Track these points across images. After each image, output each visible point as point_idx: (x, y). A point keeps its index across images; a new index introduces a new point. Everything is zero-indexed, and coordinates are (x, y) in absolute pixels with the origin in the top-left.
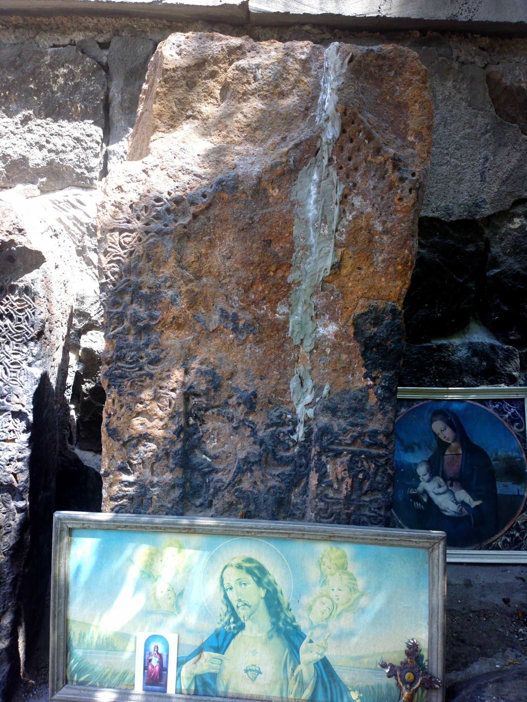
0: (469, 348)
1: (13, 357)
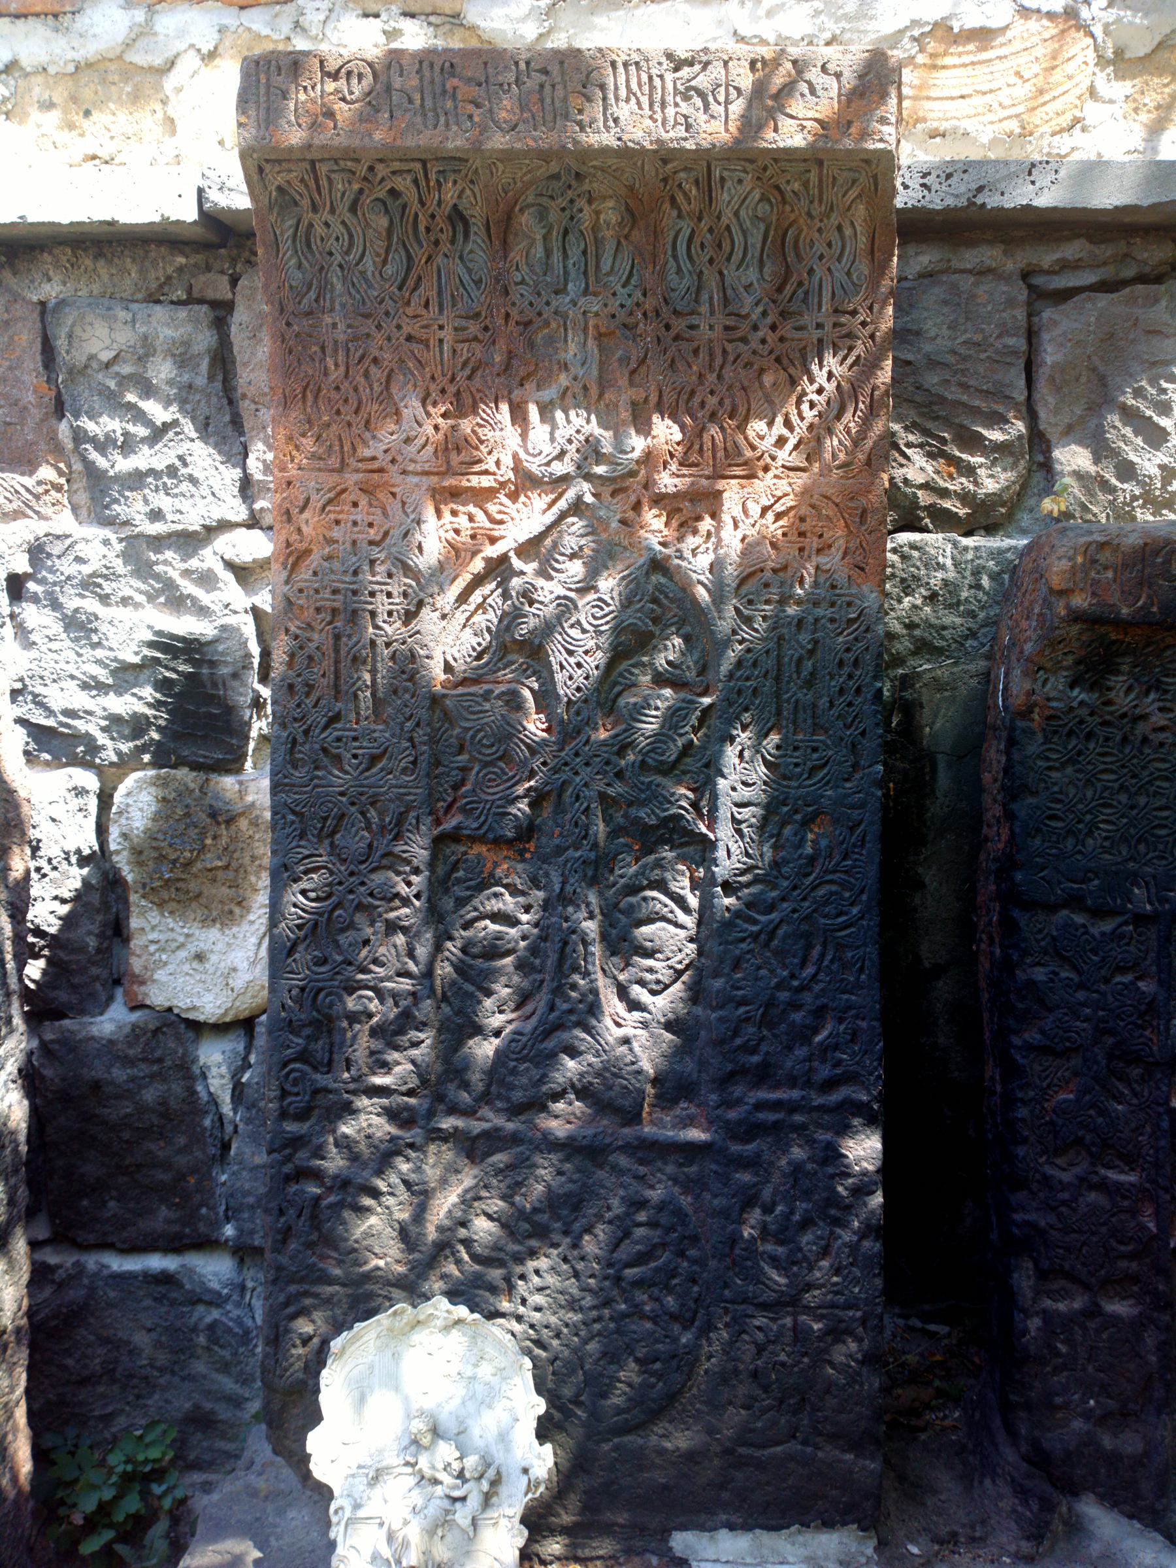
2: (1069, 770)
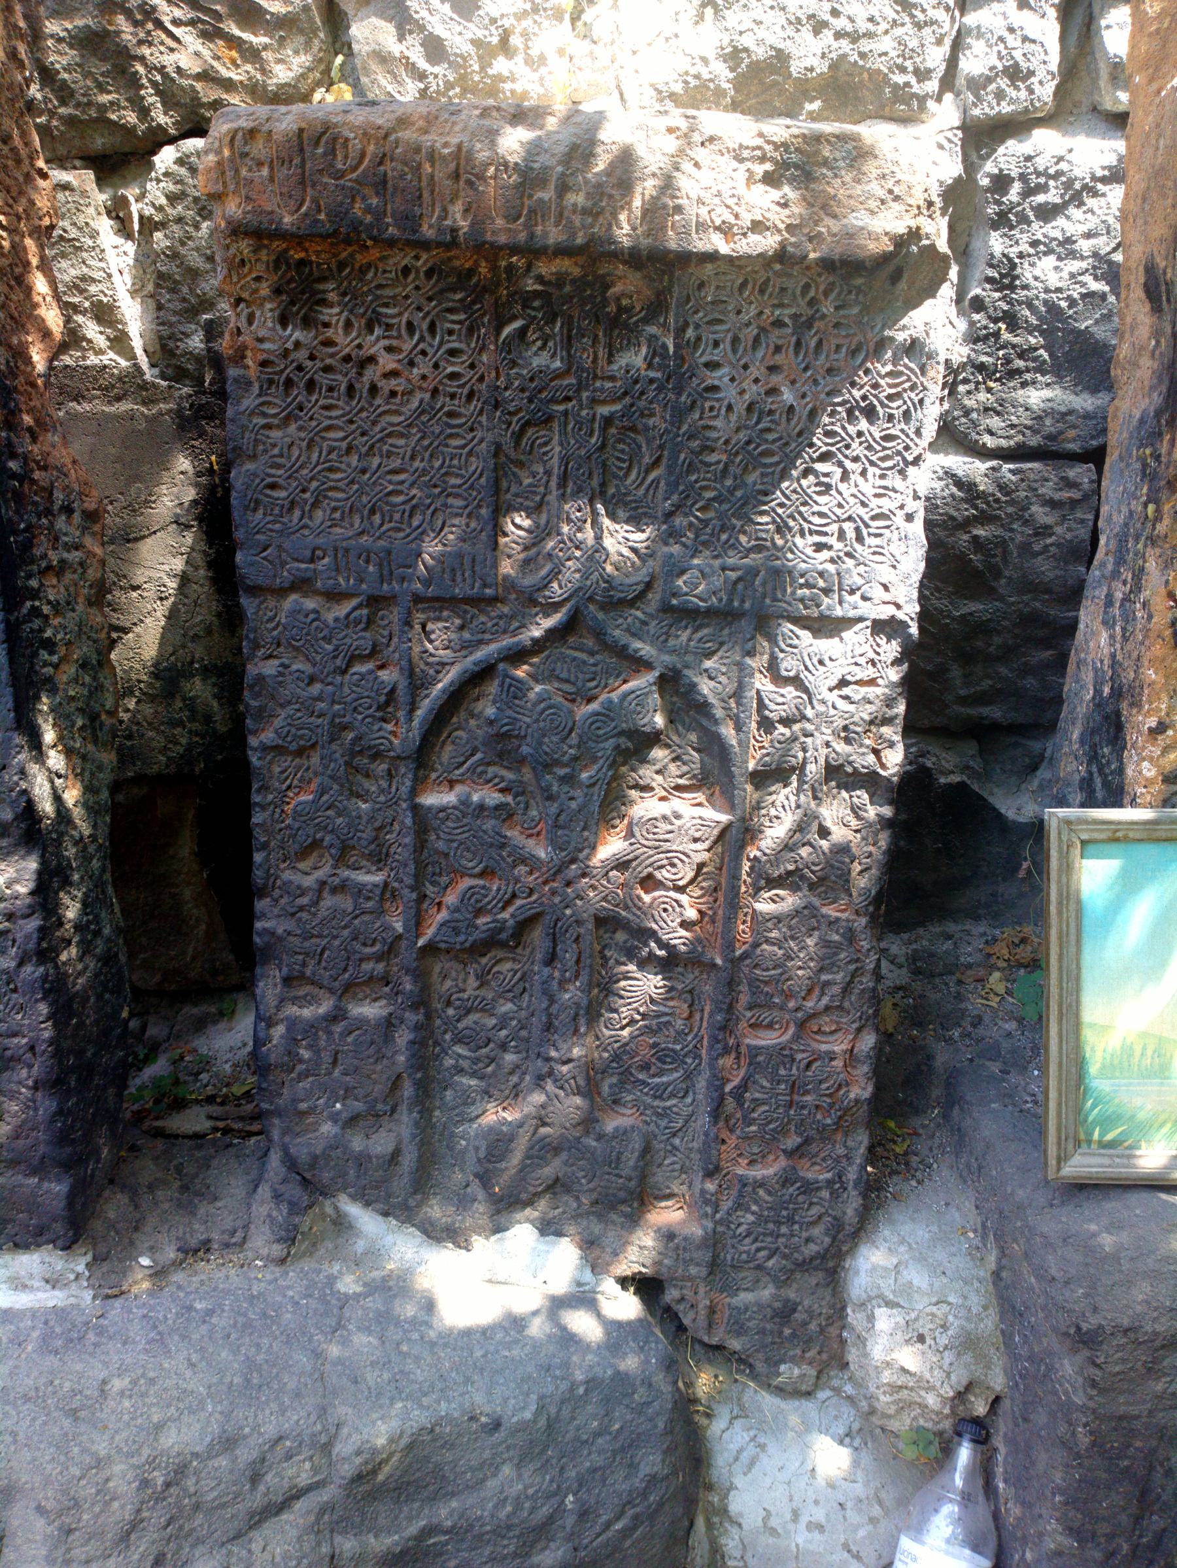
1: (874, 503)
2: (293, 428)
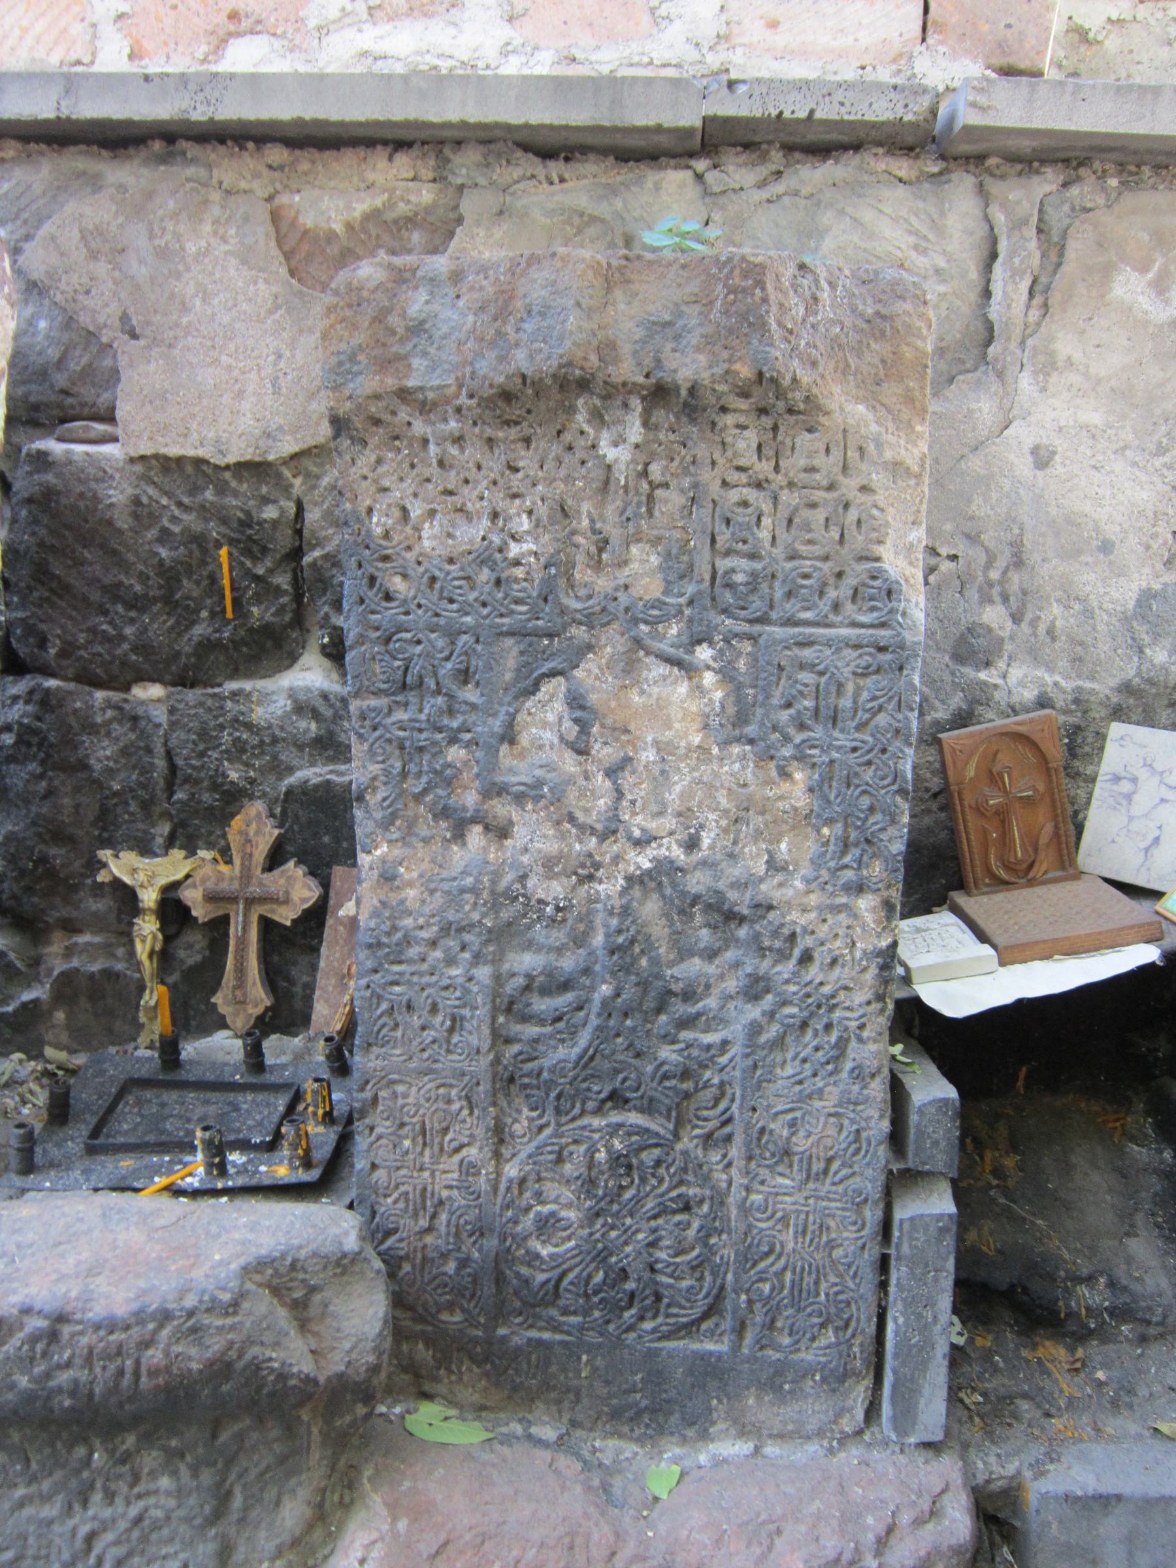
0: (290, 696)
